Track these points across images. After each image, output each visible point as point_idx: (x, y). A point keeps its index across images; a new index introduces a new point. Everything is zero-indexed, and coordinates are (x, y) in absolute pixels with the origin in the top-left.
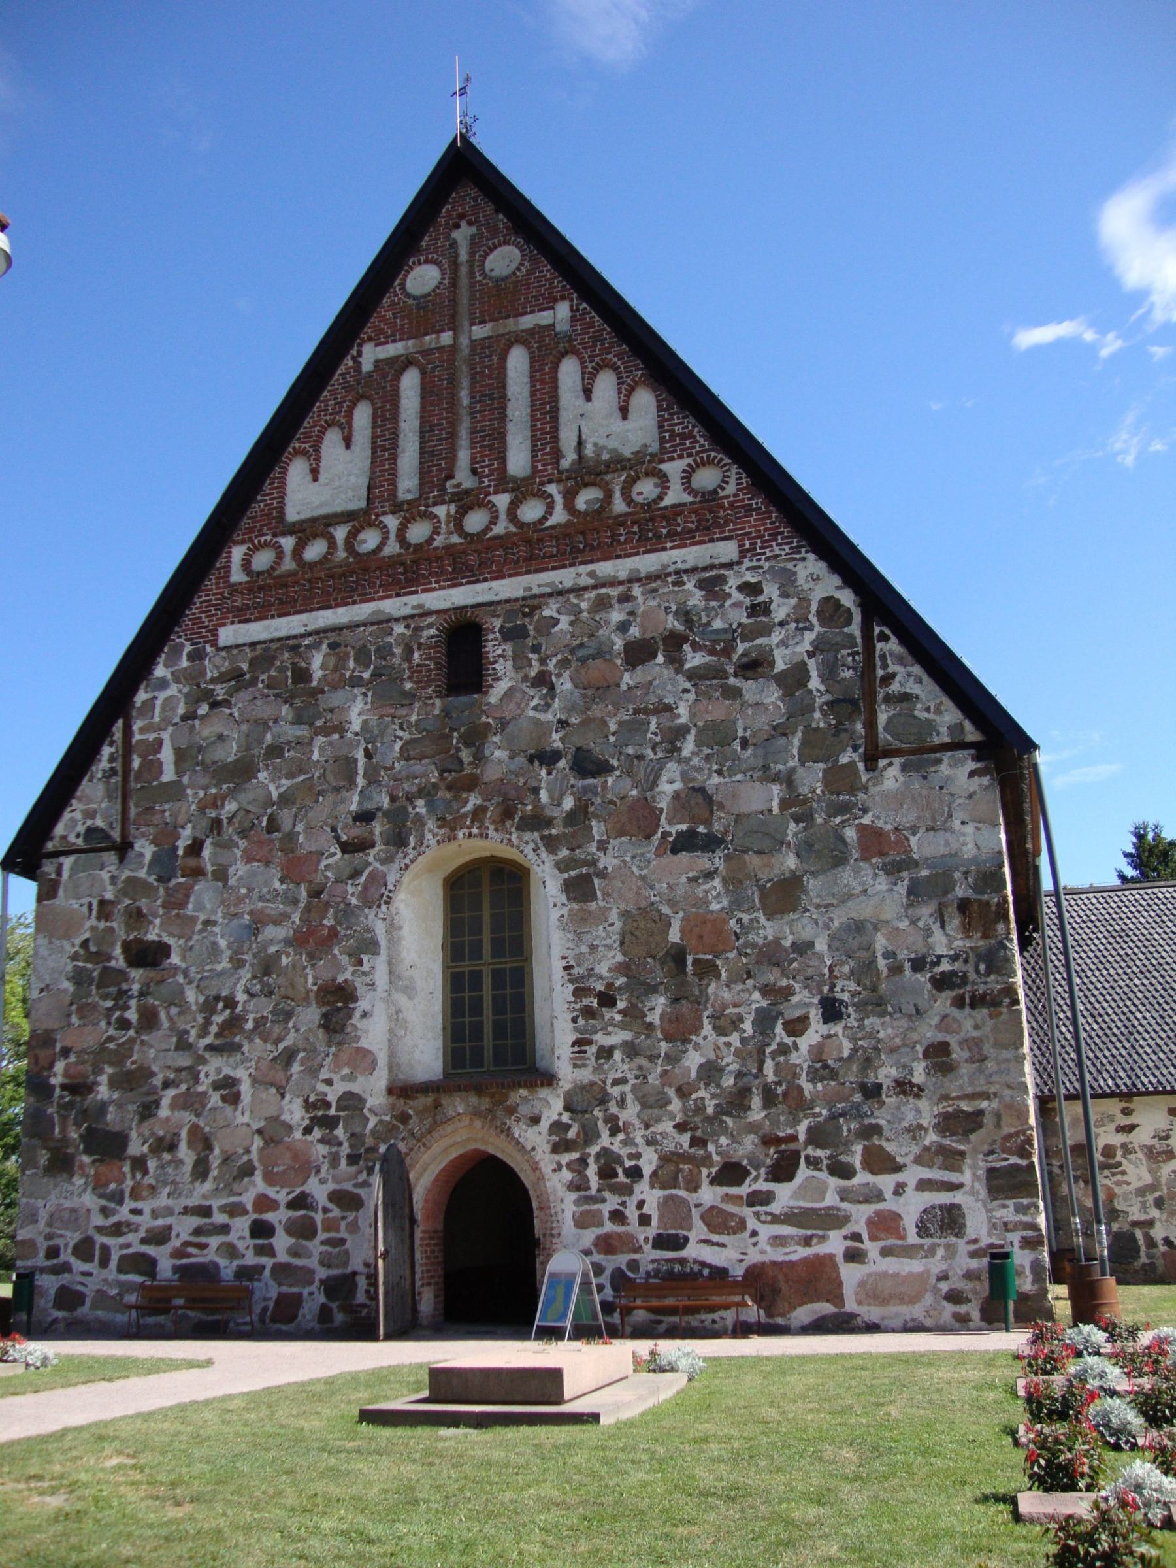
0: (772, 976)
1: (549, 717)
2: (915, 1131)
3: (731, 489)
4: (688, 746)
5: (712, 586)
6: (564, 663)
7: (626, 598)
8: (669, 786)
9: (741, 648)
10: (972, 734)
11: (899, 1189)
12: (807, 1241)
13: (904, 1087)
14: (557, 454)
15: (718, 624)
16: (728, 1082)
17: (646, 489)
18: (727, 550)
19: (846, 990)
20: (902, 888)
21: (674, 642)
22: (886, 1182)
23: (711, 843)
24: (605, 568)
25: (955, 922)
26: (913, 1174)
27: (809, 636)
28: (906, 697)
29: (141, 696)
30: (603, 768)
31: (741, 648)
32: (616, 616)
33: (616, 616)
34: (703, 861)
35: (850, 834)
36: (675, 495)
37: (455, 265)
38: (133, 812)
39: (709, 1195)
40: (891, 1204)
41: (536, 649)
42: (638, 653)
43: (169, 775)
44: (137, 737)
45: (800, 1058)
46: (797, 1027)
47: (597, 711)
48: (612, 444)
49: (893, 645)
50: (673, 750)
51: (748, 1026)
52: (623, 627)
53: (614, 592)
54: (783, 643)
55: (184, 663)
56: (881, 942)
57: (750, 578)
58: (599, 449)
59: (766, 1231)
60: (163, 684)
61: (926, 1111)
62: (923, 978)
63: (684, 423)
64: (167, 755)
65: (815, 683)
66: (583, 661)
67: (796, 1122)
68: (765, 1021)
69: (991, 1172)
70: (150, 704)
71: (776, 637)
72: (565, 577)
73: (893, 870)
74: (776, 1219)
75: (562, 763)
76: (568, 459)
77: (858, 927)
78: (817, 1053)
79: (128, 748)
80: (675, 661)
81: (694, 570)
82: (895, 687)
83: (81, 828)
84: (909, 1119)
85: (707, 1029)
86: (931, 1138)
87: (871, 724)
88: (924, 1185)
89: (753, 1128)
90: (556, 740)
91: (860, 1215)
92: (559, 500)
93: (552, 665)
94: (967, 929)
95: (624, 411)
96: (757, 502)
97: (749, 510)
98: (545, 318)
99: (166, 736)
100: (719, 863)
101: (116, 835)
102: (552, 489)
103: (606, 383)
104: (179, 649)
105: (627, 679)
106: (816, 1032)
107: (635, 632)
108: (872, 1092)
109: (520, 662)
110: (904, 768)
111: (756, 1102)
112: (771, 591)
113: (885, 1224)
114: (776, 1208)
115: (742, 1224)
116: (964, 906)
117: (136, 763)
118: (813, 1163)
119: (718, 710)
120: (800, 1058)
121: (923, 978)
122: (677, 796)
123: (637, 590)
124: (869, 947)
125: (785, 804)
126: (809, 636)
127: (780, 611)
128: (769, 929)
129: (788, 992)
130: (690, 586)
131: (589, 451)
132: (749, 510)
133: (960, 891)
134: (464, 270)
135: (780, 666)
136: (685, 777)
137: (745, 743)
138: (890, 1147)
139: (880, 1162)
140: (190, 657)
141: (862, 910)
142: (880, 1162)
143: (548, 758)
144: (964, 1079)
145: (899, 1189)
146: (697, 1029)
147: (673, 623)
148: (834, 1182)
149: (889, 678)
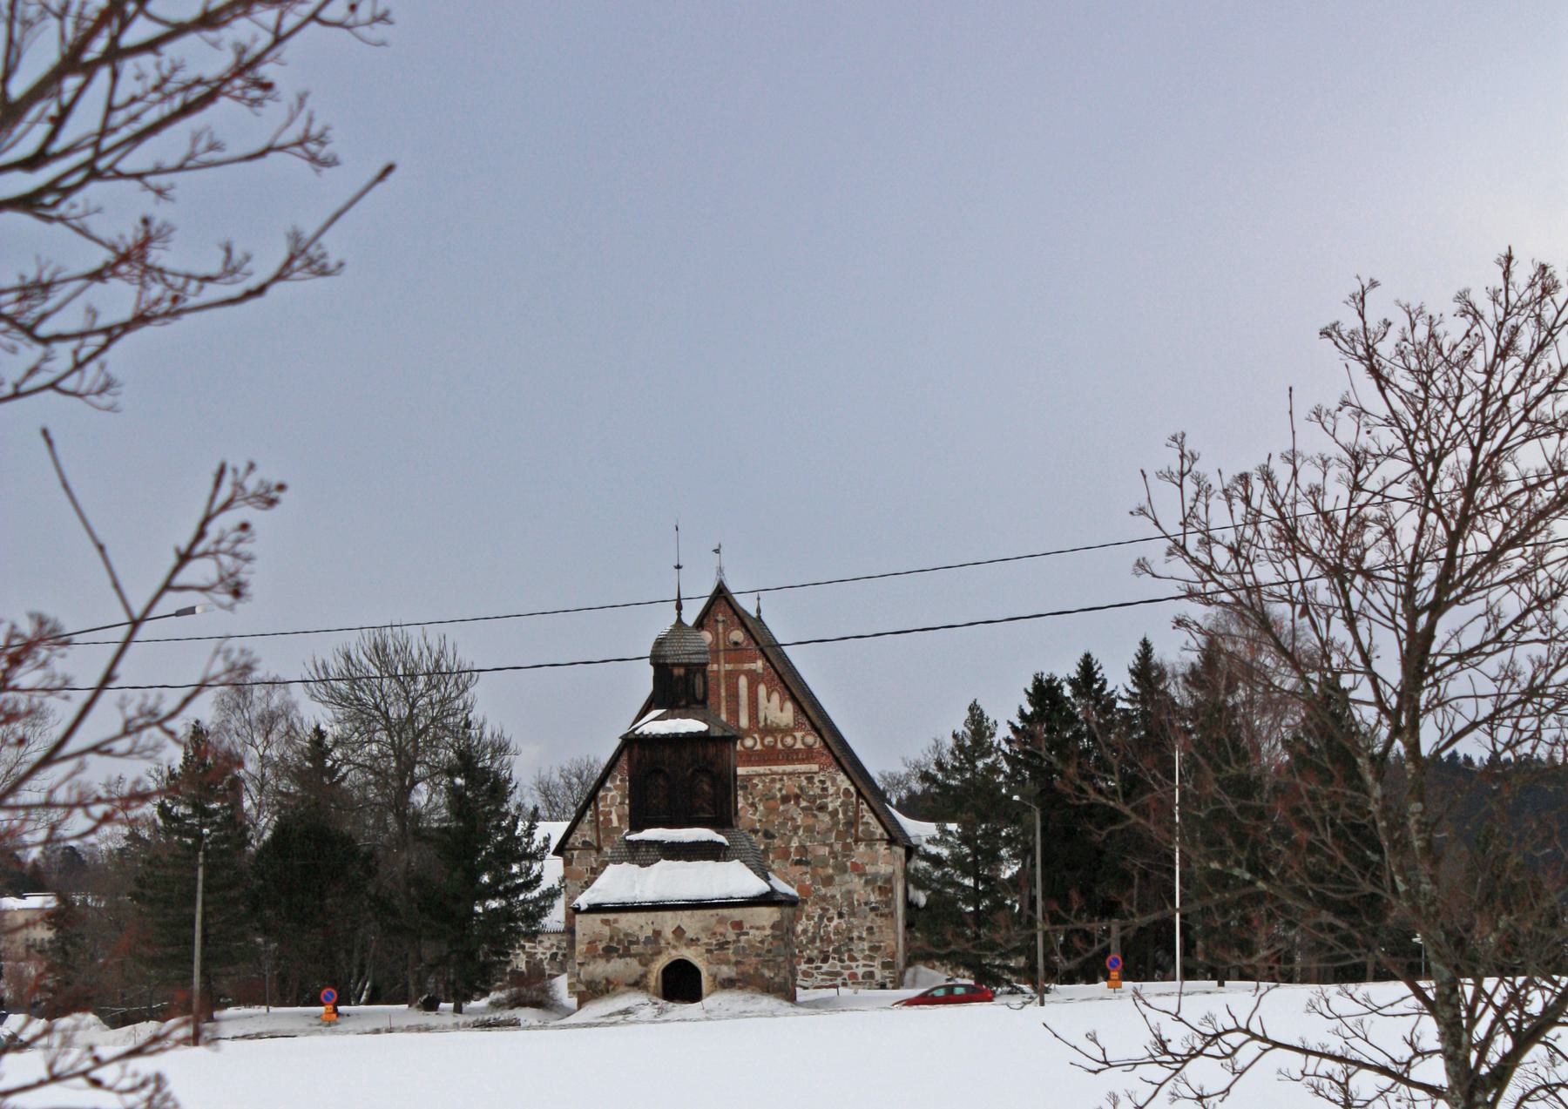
0: (824, 905)
1: (755, 818)
2: (863, 950)
3: (817, 746)
4: (801, 832)
5: (810, 780)
6: (760, 800)
7: (781, 780)
8: (795, 843)
9: (818, 801)
10: (886, 836)
11: (857, 966)
12: (831, 980)
13: (860, 938)
14: (758, 722)
15: (811, 793)
16: (810, 934)
17: (789, 740)
18: (815, 767)
19: (845, 910)
20: (863, 881)
21: (797, 797)
22: (854, 964)
23: (807, 863)
24: (775, 768)
25: (877, 892)
26: (861, 962)
27: (840, 800)
28: (868, 823)
29: (601, 793)
30: (773, 837)
31: (818, 801)
32: (778, 786)
33: (778, 786)
34: (804, 869)
35: (849, 864)
36: (799, 745)
37: (717, 634)
38: (602, 837)
39: (804, 967)
40: (855, 970)
41: (751, 794)
42: (785, 800)
43: (615, 823)
44: (601, 809)
45: (831, 929)
46: (830, 920)
47: (771, 817)
48: (777, 721)
49: (865, 806)
50: (796, 833)
51: (816, 919)
52: (780, 790)
53: (777, 777)
54: (832, 802)
55: (618, 783)
56: (856, 897)
57: (822, 778)
58: (772, 722)
59: (820, 977)
60: (609, 790)
61: (866, 945)
62: (867, 908)
63: (804, 720)
64: (614, 817)
65: (841, 816)
66: (767, 800)
67: (829, 947)
68: (821, 917)
69: (883, 963)
70: (605, 798)
71: (829, 799)
72: (761, 769)
73: (860, 876)
74: (822, 974)
75: (760, 834)
76: (762, 724)
77: (850, 892)
78: (836, 928)
79: (597, 813)
80: (797, 803)
81: (804, 773)
82: (864, 820)
83: (580, 841)
84: (861, 947)
85: (804, 919)
86: (867, 952)
87: (857, 831)
88: (864, 965)
89: (817, 948)
90: (758, 826)
91: (846, 973)
92: (758, 740)
93: (757, 799)
94: (880, 895)
95: (782, 710)
96: (826, 752)
97: (823, 754)
98: (752, 666)
99: (613, 809)
100: (809, 870)
101: (595, 844)
102: (756, 736)
103: (775, 697)
104: (615, 777)
105: (781, 808)
106: (836, 921)
107: (784, 792)
108: (851, 939)
109: (746, 798)
110: (866, 845)
111: (818, 941)
112: (828, 784)
113: (853, 976)
114: (822, 971)
115: (813, 975)
116: (880, 888)
117: (601, 818)
118: (834, 958)
119: (810, 821)
120: (831, 929)
121: (867, 908)
122: (796, 848)
123: (785, 778)
124: (852, 898)
125: (830, 853)
126: (840, 800)
127: (831, 790)
128: (823, 891)
129: (828, 910)
130: (803, 778)
131: (769, 722)
132: (823, 754)
133: (879, 884)
134: (721, 636)
135: (830, 809)
136: (800, 842)
137: (818, 833)
138: (855, 955)
139: (852, 959)
140: (621, 780)
141: (849, 886)
142: (852, 959)
143: (755, 832)
144: (877, 936)
145: (857, 966)
146: (801, 919)
147: (797, 791)
148: (839, 964)
149: (863, 817)
